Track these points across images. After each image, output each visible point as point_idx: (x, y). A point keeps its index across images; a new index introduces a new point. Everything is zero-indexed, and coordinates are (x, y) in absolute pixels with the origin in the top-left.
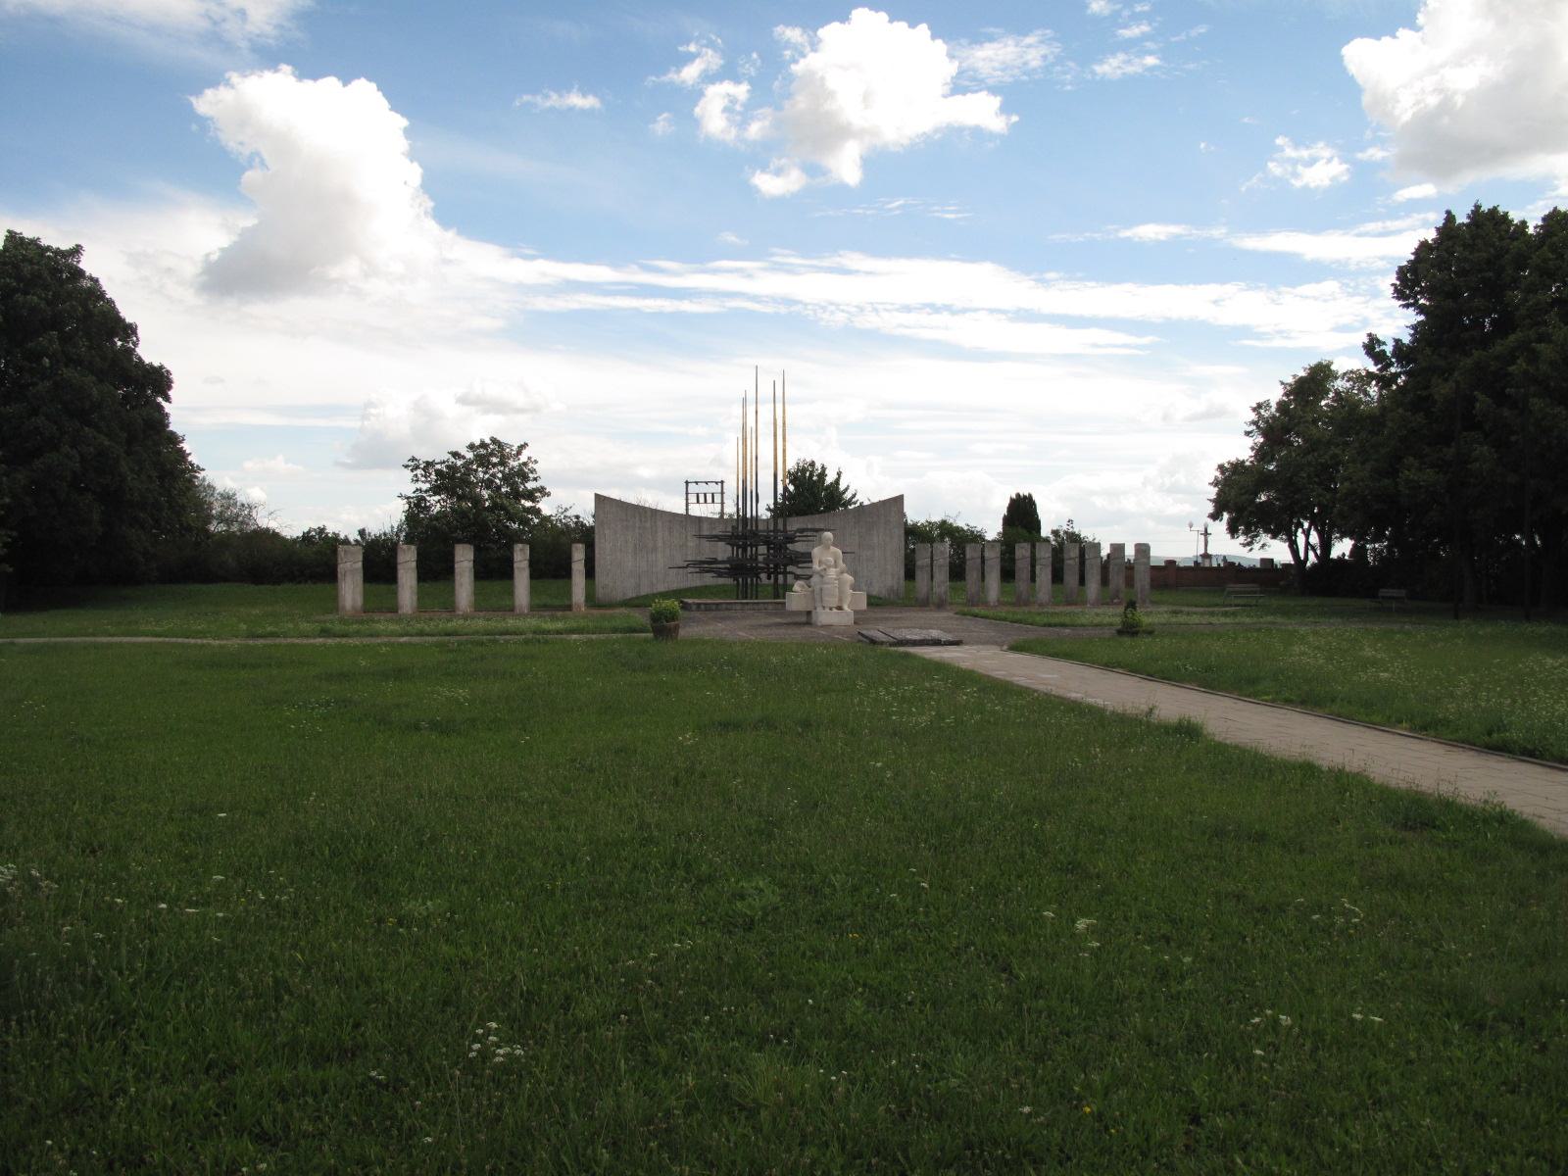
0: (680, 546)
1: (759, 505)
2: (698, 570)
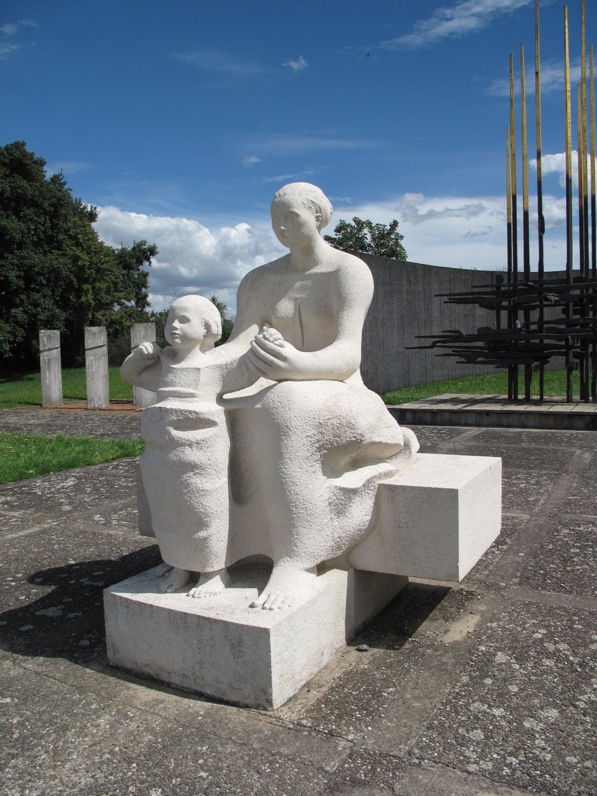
1: (545, 236)
2: (450, 351)
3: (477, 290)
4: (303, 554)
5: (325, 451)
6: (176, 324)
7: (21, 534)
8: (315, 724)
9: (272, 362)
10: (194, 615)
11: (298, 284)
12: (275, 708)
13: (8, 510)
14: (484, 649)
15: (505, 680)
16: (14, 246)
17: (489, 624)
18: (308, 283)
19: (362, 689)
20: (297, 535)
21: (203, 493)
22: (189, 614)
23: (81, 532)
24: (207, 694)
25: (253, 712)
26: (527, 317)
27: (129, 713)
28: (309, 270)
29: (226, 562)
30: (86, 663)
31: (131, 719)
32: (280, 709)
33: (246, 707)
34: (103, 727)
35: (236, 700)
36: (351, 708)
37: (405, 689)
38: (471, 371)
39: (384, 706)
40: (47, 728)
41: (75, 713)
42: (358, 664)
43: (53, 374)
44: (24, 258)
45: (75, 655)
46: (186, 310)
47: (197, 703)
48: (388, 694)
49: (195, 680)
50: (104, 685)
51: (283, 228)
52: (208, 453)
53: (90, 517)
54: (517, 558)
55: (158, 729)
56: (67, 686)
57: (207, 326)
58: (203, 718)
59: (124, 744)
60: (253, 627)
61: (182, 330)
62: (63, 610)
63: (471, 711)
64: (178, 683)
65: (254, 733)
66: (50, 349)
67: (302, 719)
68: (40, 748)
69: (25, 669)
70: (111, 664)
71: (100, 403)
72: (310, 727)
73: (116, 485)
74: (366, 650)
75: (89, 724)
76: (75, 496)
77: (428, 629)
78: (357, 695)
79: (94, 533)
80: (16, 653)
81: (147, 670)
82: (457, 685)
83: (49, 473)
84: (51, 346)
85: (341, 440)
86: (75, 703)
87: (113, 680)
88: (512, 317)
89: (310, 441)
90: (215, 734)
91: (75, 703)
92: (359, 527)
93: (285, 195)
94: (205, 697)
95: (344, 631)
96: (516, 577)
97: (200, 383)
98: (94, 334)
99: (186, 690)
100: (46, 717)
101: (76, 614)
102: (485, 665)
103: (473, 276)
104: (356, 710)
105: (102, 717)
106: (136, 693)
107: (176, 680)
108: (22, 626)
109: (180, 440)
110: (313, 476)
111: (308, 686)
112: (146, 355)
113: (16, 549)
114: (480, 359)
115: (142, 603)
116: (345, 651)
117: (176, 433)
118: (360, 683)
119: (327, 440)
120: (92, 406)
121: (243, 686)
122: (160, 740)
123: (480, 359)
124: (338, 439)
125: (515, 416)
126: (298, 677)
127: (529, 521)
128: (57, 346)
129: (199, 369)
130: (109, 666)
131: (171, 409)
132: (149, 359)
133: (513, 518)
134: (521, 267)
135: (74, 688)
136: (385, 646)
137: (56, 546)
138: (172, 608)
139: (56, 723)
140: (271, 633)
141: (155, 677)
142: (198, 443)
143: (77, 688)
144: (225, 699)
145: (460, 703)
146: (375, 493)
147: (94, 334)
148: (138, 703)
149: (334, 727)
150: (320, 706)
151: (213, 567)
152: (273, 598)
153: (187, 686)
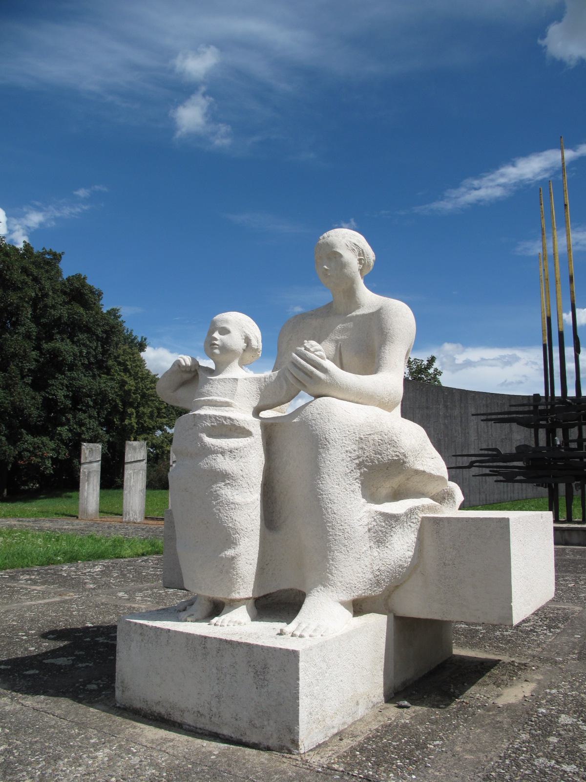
2: (487, 471)
3: (513, 409)
4: (339, 584)
5: (365, 469)
6: (216, 335)
7: (40, 602)
8: (348, 769)
9: (312, 372)
10: (215, 638)
11: (339, 327)
12: (302, 752)
13: (30, 585)
14: (544, 711)
15: (573, 739)
16: (66, 367)
17: (548, 691)
18: (350, 325)
19: (403, 741)
20: (333, 561)
21: (233, 506)
22: (209, 637)
23: (102, 604)
24: (223, 735)
25: (275, 755)
26: (565, 435)
27: (132, 749)
28: (351, 313)
29: (253, 591)
30: (91, 703)
31: (134, 754)
32: (307, 754)
33: (268, 749)
34: (101, 759)
35: (256, 742)
36: (391, 756)
37: (453, 742)
38: (509, 496)
39: (430, 757)
40: (37, 756)
41: (71, 745)
42: (398, 718)
43: (91, 486)
44: (74, 379)
45: (80, 696)
46: (227, 321)
47: (211, 744)
48: (434, 746)
49: (211, 718)
50: (107, 723)
51: (326, 267)
52: (242, 464)
53: (114, 593)
54: (572, 639)
55: (164, 764)
56: (66, 722)
57: (247, 340)
58: (217, 758)
59: (122, 776)
60: (281, 649)
61: (221, 340)
62: (73, 660)
63: (536, 766)
64: (192, 723)
65: (276, 774)
66: (91, 462)
67: (333, 763)
68: (25, 773)
69: (23, 705)
70: (118, 705)
71: (135, 517)
72: (342, 771)
73: (144, 573)
74: (407, 707)
75: (85, 756)
76: (100, 578)
77: (476, 692)
78: (397, 745)
79: (116, 606)
80: (16, 692)
82: (516, 742)
83: (77, 562)
84: (92, 459)
85: (383, 458)
86: (72, 737)
87: (119, 719)
88: (551, 433)
89: (350, 457)
90: (230, 773)
91: (72, 737)
92: (401, 563)
93: (328, 237)
94: (220, 738)
95: (382, 685)
96: (574, 653)
97: (236, 394)
98: (135, 449)
99: (200, 732)
100: (37, 746)
101: (87, 664)
102: (548, 725)
104: (397, 759)
105: (101, 751)
106: (142, 731)
107: (189, 720)
108: (27, 670)
109: (212, 447)
110: (352, 495)
111: (340, 735)
112: (183, 366)
113: (33, 612)
114: (518, 478)
115: (159, 628)
116: (383, 708)
117: (208, 440)
118: (401, 735)
119: (367, 457)
120: (127, 520)
121: (266, 723)
122: (165, 774)
123: (518, 478)
124: (380, 457)
126: (328, 722)
127: (581, 612)
128: (98, 460)
129: (236, 380)
130: (117, 707)
132: (186, 372)
133: (564, 609)
134: (558, 393)
135: (73, 724)
136: (429, 705)
137: (74, 613)
138: (191, 632)
139: (48, 753)
140: (300, 656)
141: (165, 717)
142: (231, 452)
143: (77, 724)
144: (244, 740)
145: (522, 757)
146: (418, 527)
147: (135, 449)
148: (144, 740)
149: (371, 773)
150: (355, 753)
151: (239, 593)
152: (304, 626)
153: (202, 726)
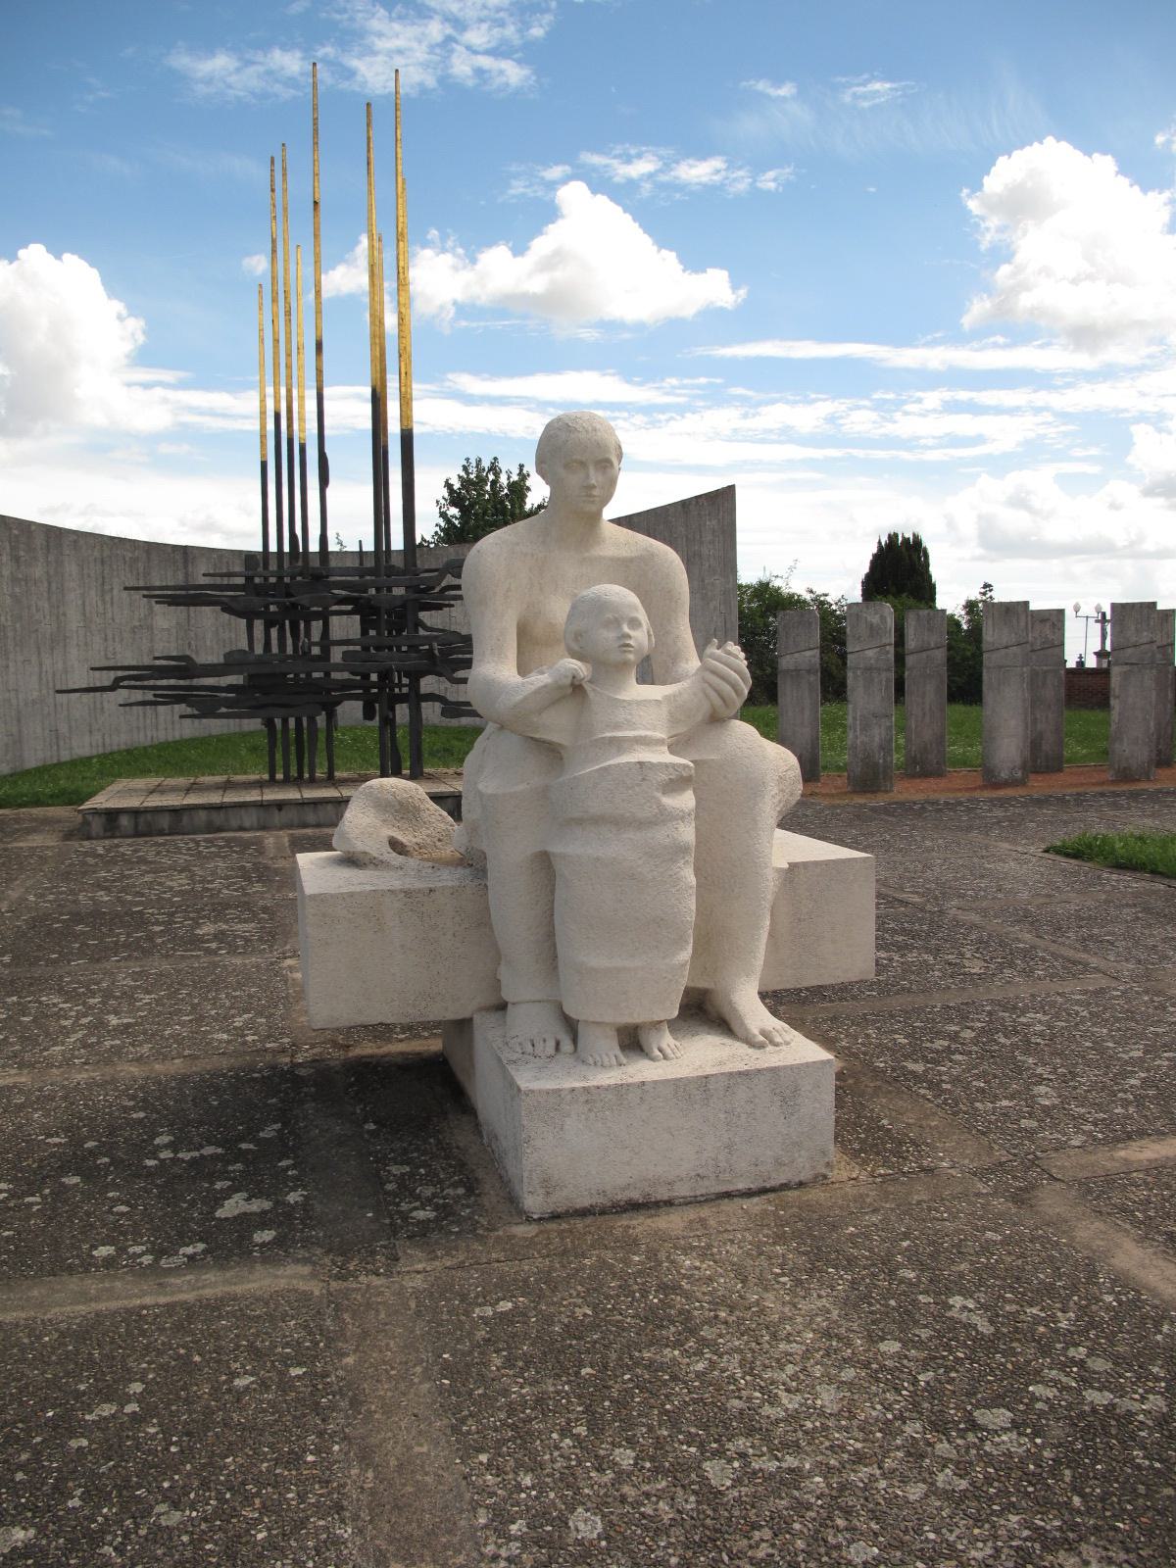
0: (133, 630)
1: (329, 491)
2: (149, 696)
38: (149, 734)
69: (418, 1272)
70: (535, 1217)
81: (623, 1197)
103: (148, 552)
107: (683, 1190)
114: (223, 710)
125: (330, 807)
131: (660, 764)
138: (679, 1076)
144: (768, 1186)
153: (704, 1192)
